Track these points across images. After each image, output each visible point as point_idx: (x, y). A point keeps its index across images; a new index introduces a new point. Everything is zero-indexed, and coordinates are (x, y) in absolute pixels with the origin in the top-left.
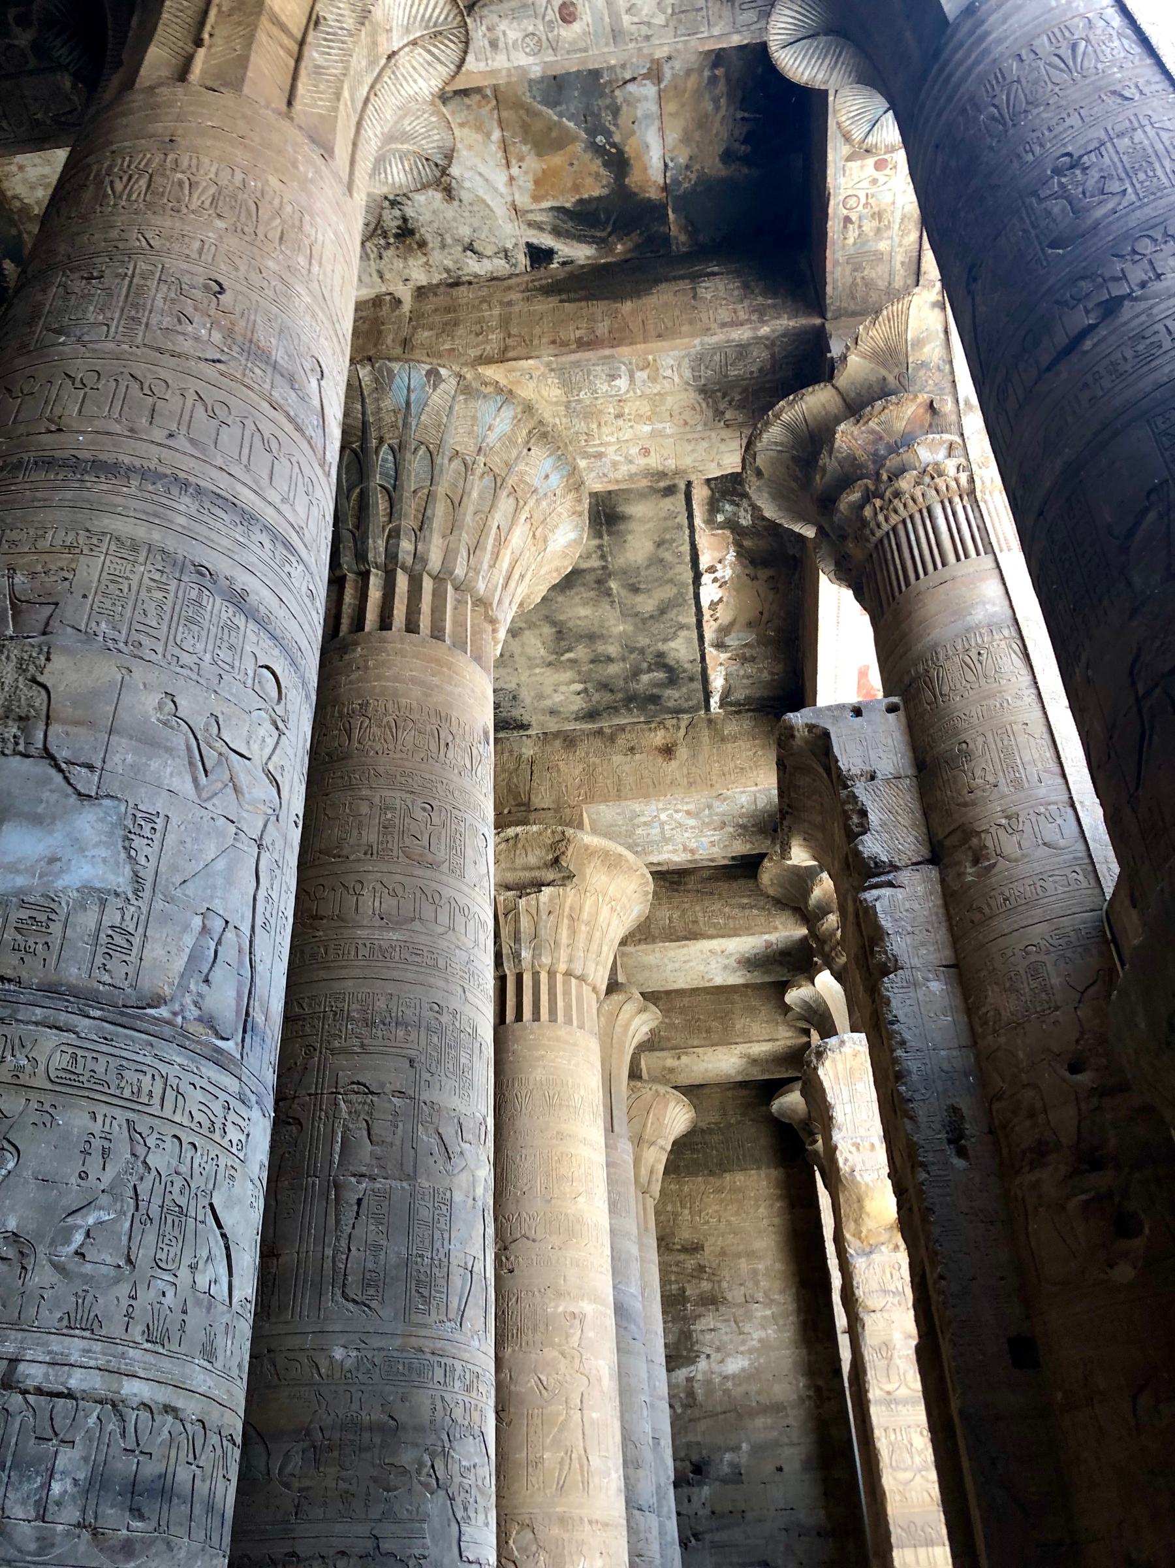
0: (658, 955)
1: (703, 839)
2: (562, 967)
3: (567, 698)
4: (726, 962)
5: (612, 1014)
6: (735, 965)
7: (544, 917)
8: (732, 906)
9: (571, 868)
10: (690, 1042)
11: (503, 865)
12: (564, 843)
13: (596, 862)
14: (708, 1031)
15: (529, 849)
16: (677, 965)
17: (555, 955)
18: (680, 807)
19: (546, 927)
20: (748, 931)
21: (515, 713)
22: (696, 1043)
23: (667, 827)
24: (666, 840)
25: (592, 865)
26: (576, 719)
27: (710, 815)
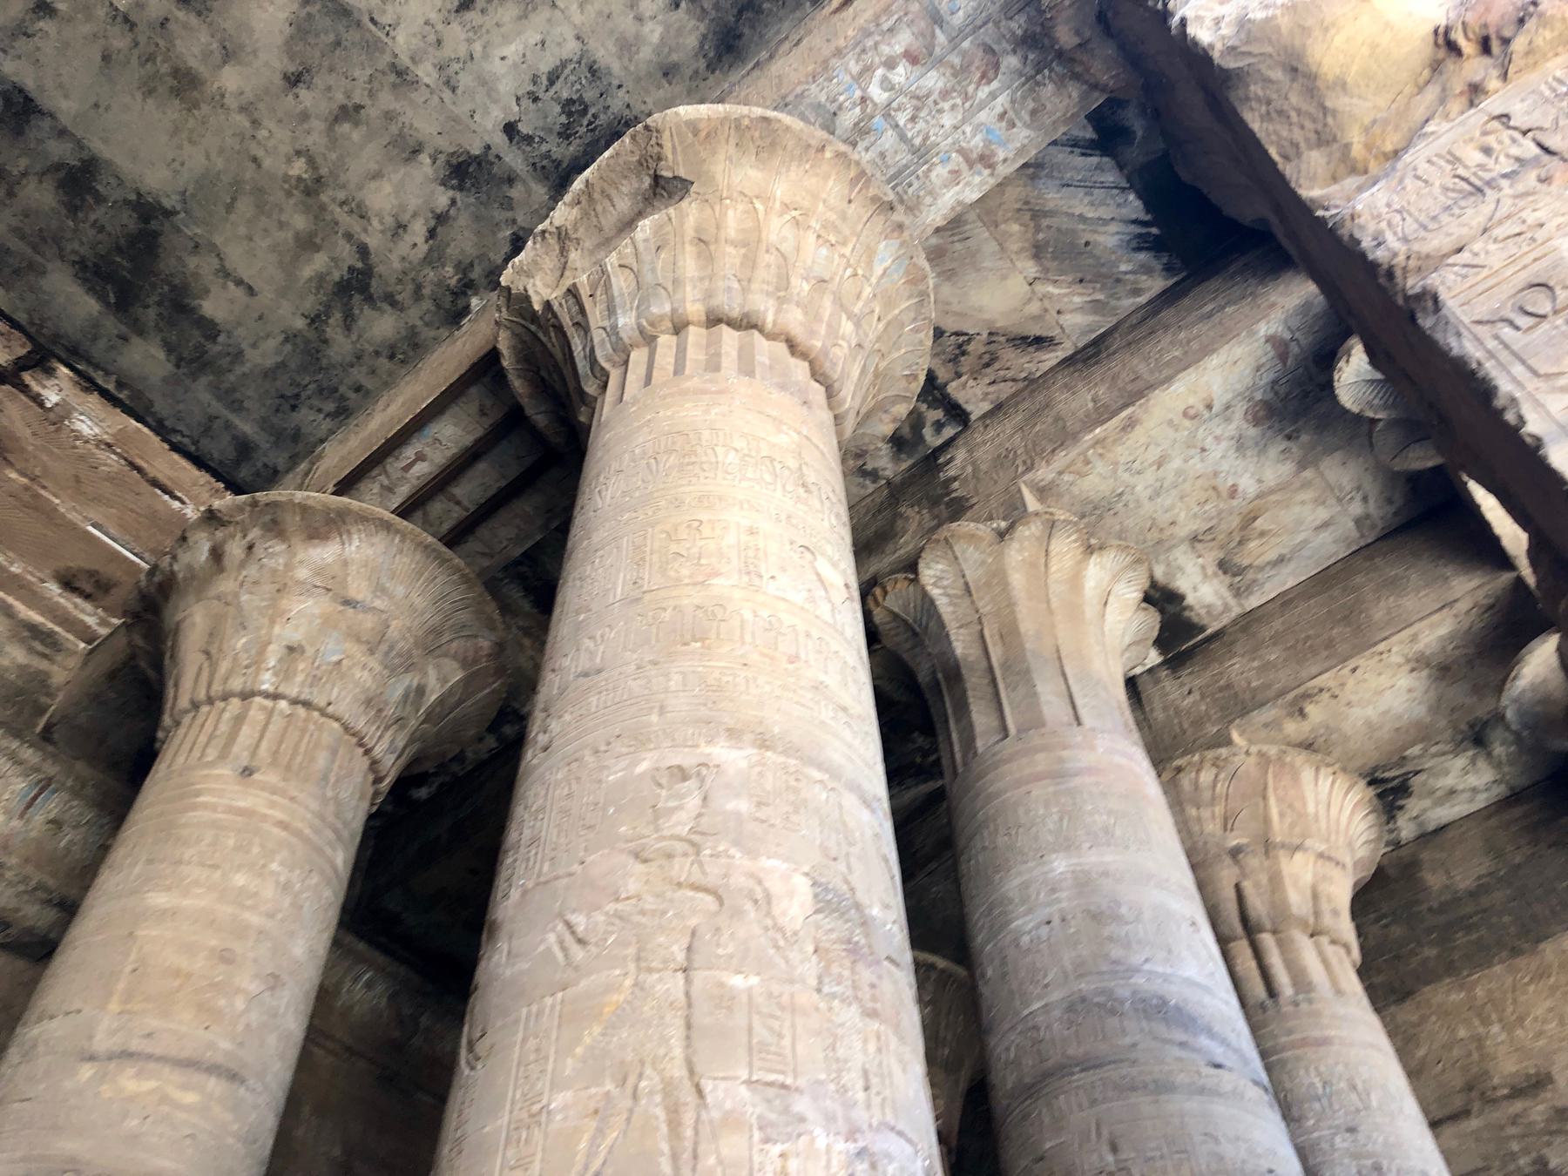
0: (1100, 467)
1: (983, 116)
2: (694, 308)
3: (667, 28)
4: (1231, 429)
5: (1033, 565)
6: (1253, 432)
7: (647, 258)
8: (1194, 324)
9: (682, 173)
10: (1304, 674)
11: (588, 244)
12: (653, 141)
13: (727, 150)
14: (1330, 644)
15: (613, 193)
16: (1150, 476)
17: (678, 296)
18: (885, 50)
19: (653, 270)
20: (1226, 336)
21: (617, 102)
22: (1314, 670)
23: (902, 119)
24: (922, 153)
25: (721, 157)
26: (711, 67)
27: (954, 42)
